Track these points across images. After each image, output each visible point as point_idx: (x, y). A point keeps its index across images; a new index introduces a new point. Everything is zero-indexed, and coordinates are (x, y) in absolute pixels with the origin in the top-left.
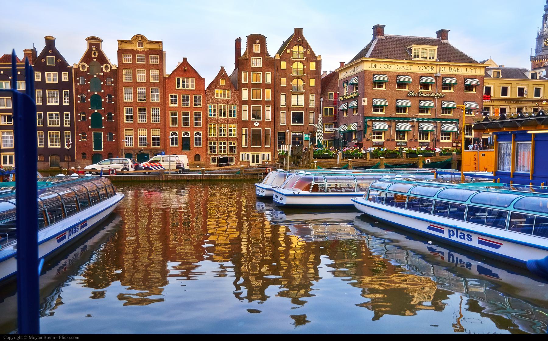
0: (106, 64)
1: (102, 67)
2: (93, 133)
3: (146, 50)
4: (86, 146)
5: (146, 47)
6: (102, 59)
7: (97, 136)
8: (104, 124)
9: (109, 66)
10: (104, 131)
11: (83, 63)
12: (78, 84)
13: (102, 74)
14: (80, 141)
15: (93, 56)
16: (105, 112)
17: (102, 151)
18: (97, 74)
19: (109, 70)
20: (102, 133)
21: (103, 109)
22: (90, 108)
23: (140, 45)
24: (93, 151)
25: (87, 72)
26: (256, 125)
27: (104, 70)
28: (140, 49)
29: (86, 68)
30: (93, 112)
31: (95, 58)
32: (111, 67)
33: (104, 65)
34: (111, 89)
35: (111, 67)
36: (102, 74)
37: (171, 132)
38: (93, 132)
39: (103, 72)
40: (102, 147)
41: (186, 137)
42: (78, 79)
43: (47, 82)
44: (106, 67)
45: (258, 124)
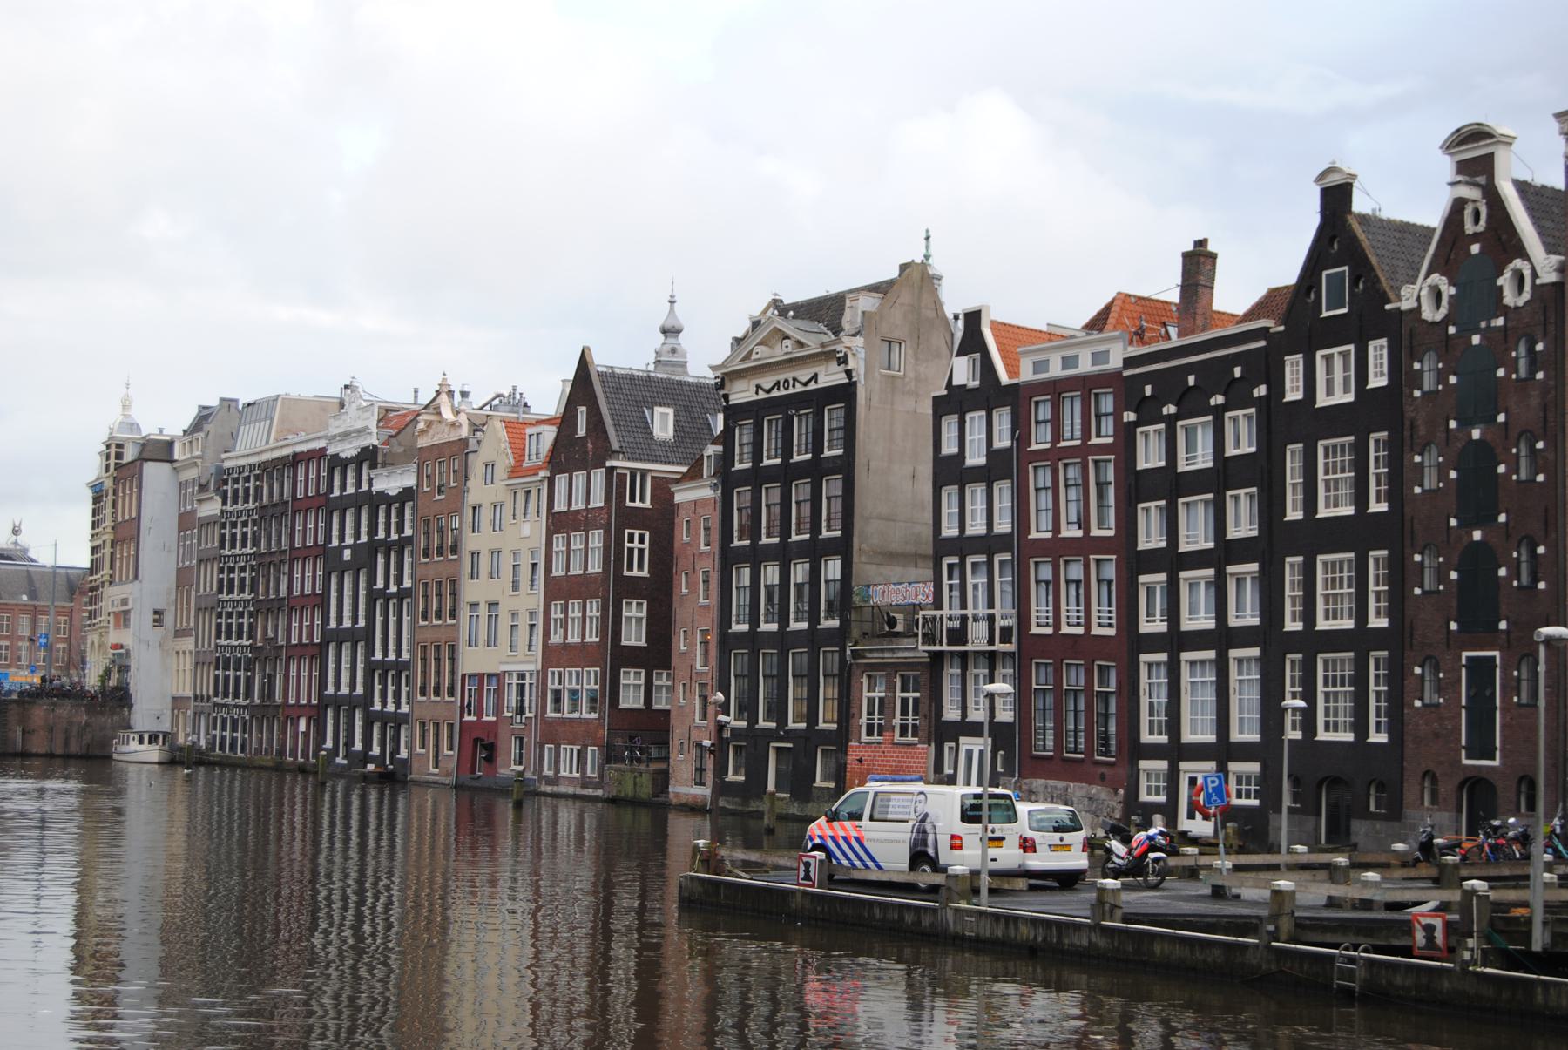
0: (1518, 263)
2: (1464, 662)
4: (1437, 735)
6: (1504, 237)
7: (1481, 670)
8: (1503, 609)
9: (1527, 273)
11: (1436, 278)
12: (1417, 393)
13: (1500, 322)
15: (1470, 228)
16: (1508, 536)
17: (1496, 763)
18: (1483, 324)
19: (1526, 296)
20: (1498, 661)
21: (1502, 518)
22: (1453, 522)
24: (1466, 762)
25: (1446, 321)
27: (1509, 298)
29: (1445, 302)
30: (1465, 541)
31: (1476, 237)
32: (1535, 275)
33: (1508, 274)
34: (1535, 401)
35: (1535, 275)
36: (1500, 322)
38: (1465, 654)
39: (1505, 311)
40: (1498, 744)
42: (1417, 366)
43: (1322, 401)
44: (1519, 278)
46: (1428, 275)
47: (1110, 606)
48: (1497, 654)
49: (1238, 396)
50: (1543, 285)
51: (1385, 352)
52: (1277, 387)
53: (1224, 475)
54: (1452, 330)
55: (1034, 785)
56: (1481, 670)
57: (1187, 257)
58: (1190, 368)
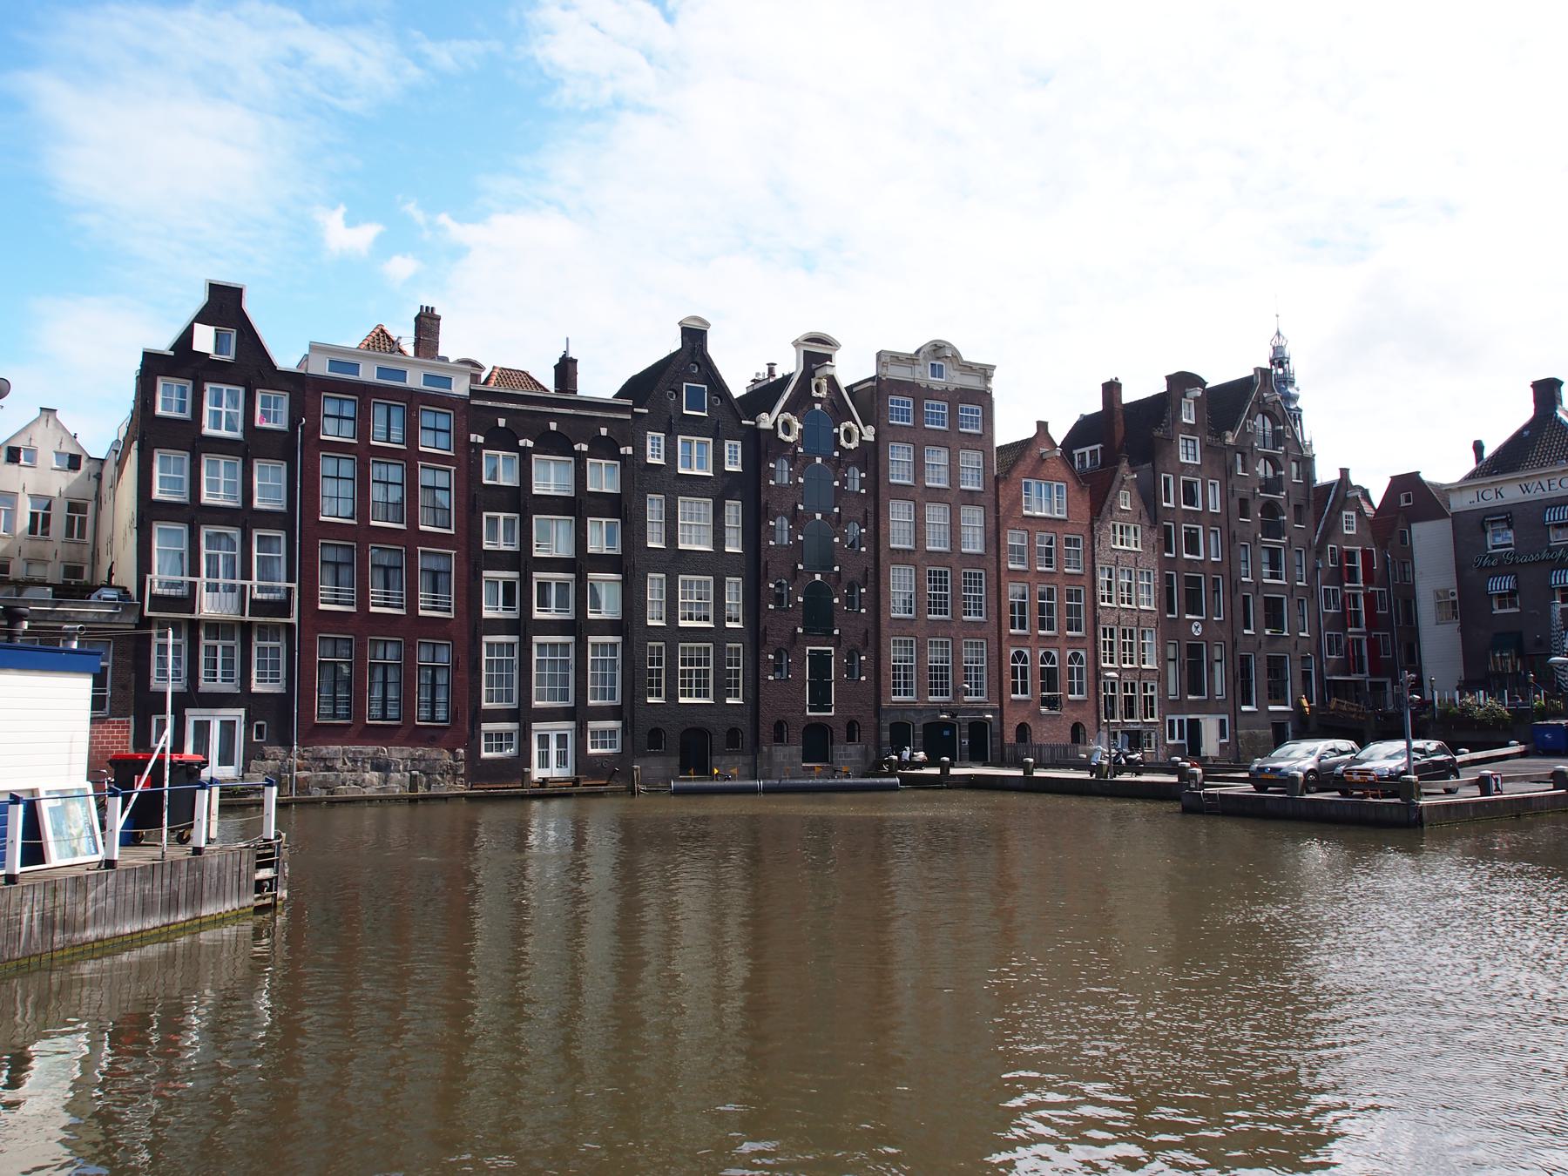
0: (849, 424)
1: (836, 430)
3: (951, 389)
5: (954, 380)
7: (820, 662)
10: (837, 647)
11: (787, 415)
12: (772, 483)
14: (771, 678)
15: (814, 393)
17: (832, 713)
23: (936, 371)
24: (808, 713)
26: (1197, 634)
27: (843, 442)
28: (937, 383)
31: (819, 400)
32: (861, 434)
35: (861, 434)
37: (1012, 651)
41: (1048, 666)
45: (1200, 629)
46: (782, 411)
47: (738, 600)
48: (832, 648)
49: (605, 448)
50: (865, 441)
51: (739, 450)
52: (640, 450)
53: (578, 506)
54: (800, 450)
55: (325, 751)
56: (820, 662)
57: (418, 319)
58: (554, 416)
